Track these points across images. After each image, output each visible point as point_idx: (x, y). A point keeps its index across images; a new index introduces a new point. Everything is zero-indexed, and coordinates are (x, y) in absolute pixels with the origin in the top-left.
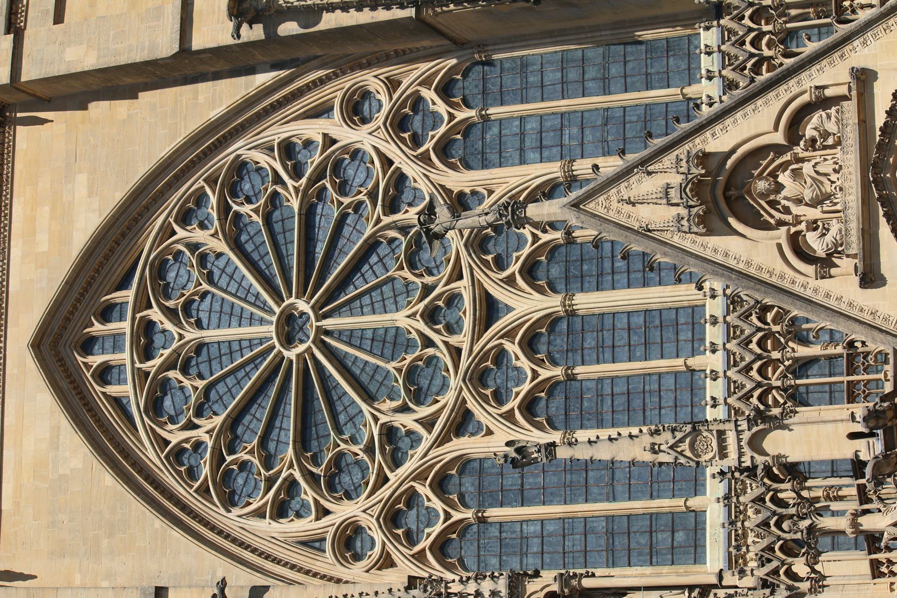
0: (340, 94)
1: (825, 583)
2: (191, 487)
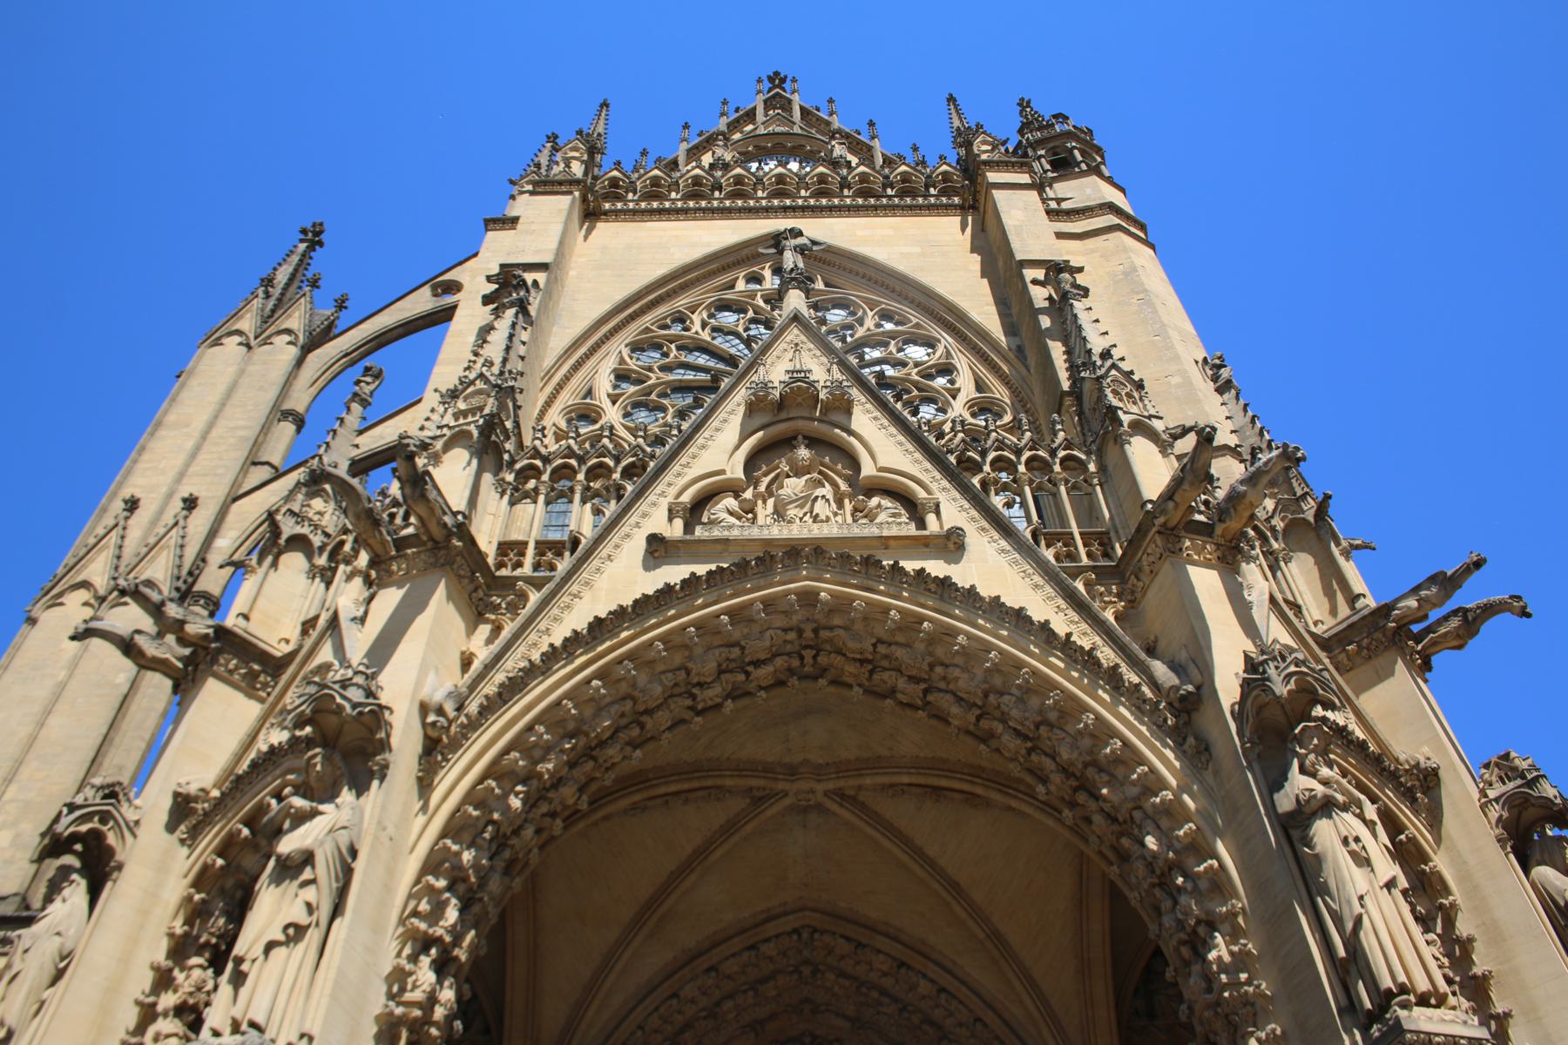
0: (998, 396)
1: (318, 580)
2: (652, 325)
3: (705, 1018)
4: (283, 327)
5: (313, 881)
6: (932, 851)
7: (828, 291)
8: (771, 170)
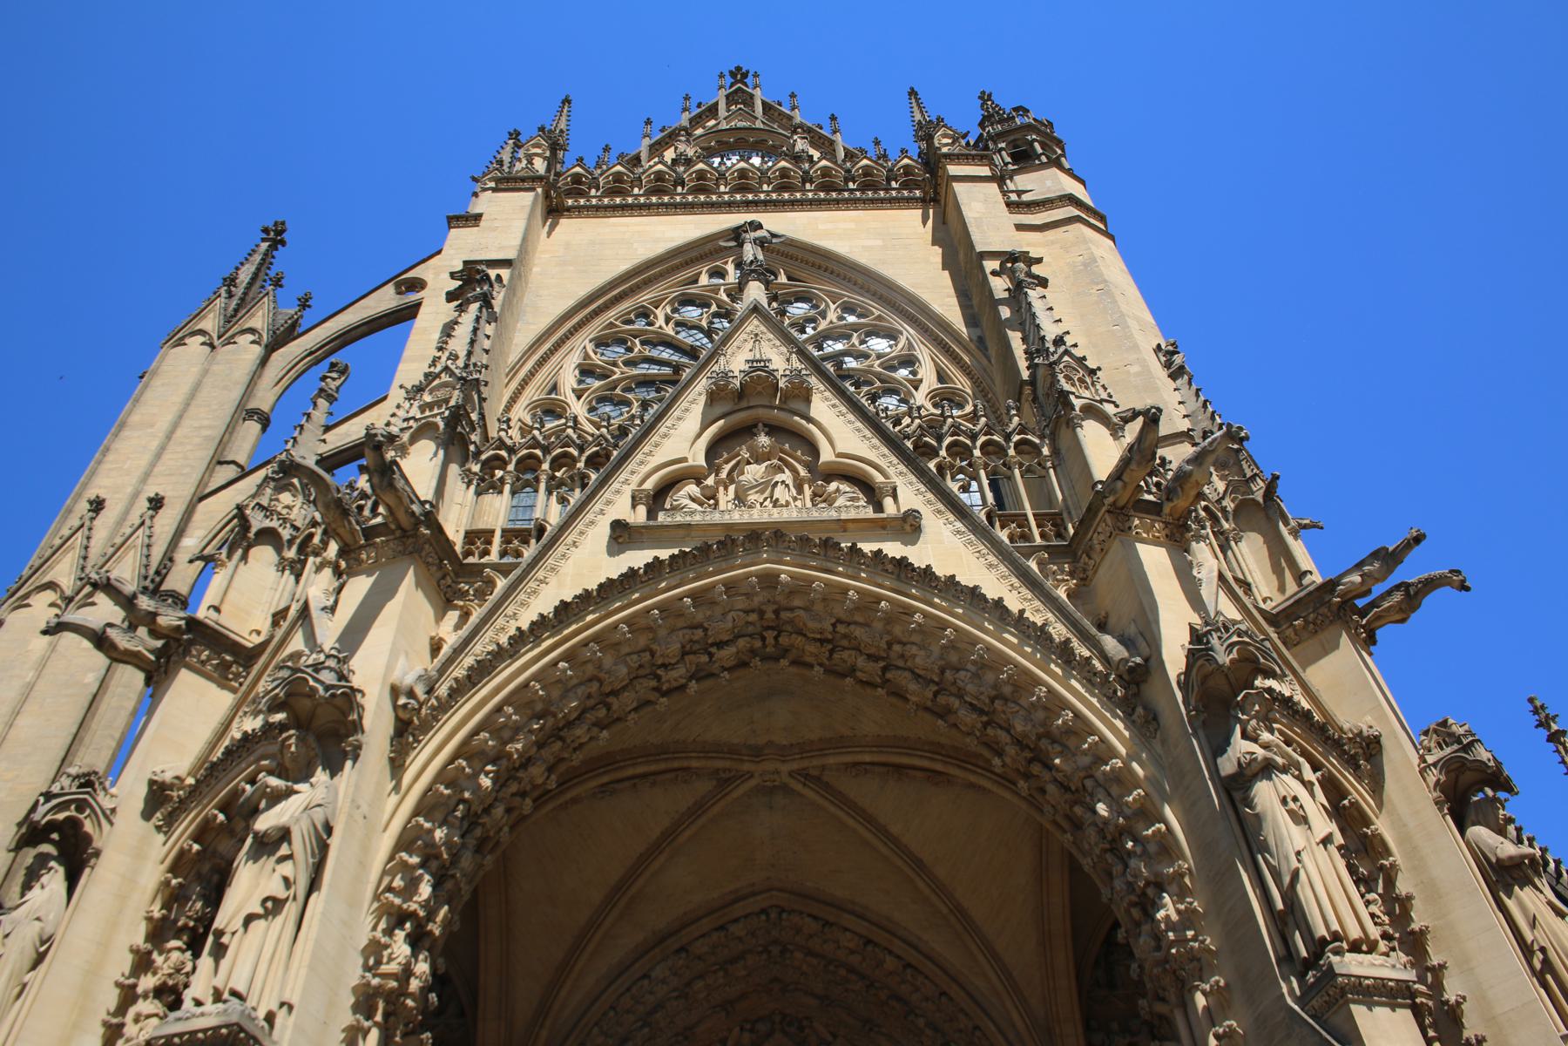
0: (960, 387)
1: (287, 572)
2: (616, 320)
3: (677, 998)
4: (247, 326)
5: (290, 857)
6: (895, 829)
7: (791, 285)
8: (734, 165)
